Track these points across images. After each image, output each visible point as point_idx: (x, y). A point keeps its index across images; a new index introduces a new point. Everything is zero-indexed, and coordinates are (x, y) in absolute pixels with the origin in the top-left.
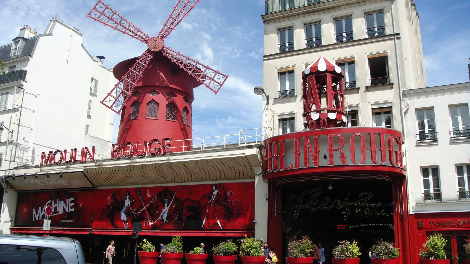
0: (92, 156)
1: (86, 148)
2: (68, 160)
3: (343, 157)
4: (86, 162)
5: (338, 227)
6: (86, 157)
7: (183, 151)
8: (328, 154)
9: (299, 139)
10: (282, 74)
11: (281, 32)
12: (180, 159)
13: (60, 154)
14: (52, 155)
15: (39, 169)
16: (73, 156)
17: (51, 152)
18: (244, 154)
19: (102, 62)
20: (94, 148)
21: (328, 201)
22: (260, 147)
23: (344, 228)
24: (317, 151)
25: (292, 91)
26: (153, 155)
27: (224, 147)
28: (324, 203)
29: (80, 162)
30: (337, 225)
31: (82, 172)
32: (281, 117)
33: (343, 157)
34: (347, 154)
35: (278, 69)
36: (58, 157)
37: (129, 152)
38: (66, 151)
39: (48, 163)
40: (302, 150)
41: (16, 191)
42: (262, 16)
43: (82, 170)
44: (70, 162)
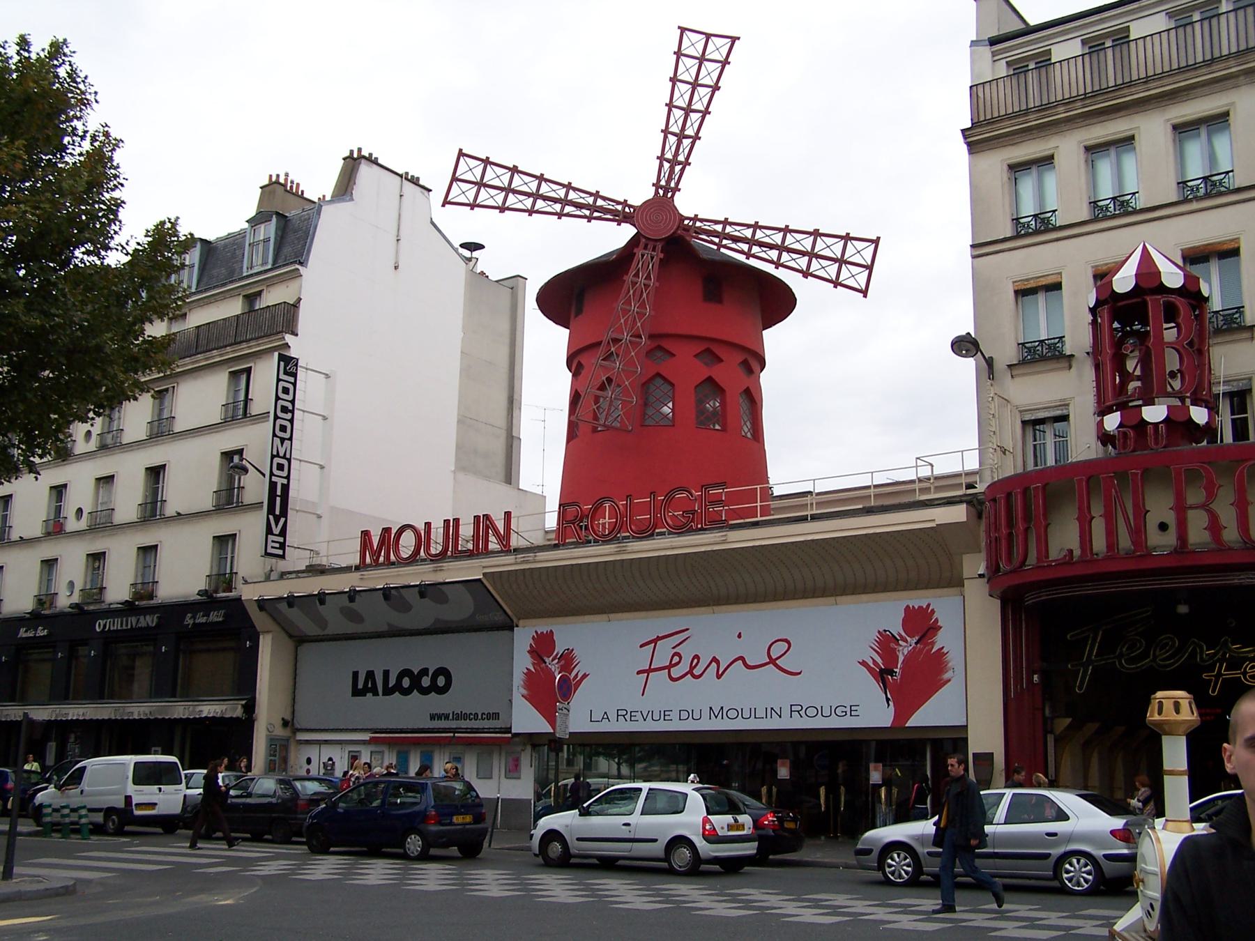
0: (504, 539)
1: (487, 517)
2: (436, 549)
3: (1215, 527)
4: (487, 553)
6: (487, 541)
7: (757, 517)
8: (1170, 518)
9: (1088, 482)
10: (1024, 293)
11: (1017, 173)
12: (754, 540)
13: (412, 533)
14: (389, 538)
15: (357, 575)
16: (451, 540)
17: (387, 531)
18: (934, 520)
19: (477, 259)
20: (508, 515)
21: (1170, 643)
22: (973, 502)
24: (1141, 513)
25: (1058, 342)
26: (681, 529)
27: (872, 504)
28: (1160, 651)
29: (470, 554)
31: (479, 580)
32: (1027, 418)
33: (1215, 527)
34: (1228, 516)
35: (1015, 282)
36: (407, 543)
37: (604, 524)
38: (428, 525)
39: (381, 559)
40: (1097, 509)
41: (291, 636)
42: (963, 131)
43: (481, 577)
44: (442, 556)
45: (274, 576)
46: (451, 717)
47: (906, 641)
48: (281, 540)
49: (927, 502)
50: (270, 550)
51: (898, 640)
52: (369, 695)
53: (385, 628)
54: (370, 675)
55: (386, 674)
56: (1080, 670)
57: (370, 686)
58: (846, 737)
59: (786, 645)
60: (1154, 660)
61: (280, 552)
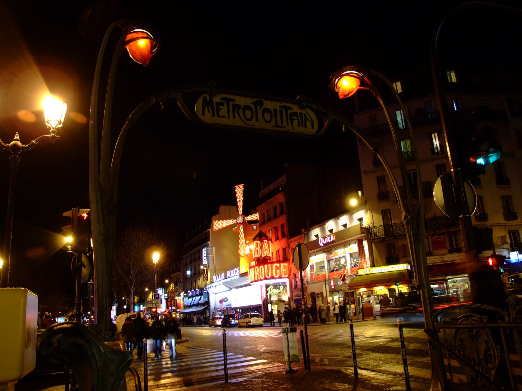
48: (207, 278)
50: (205, 280)
58: (255, 306)
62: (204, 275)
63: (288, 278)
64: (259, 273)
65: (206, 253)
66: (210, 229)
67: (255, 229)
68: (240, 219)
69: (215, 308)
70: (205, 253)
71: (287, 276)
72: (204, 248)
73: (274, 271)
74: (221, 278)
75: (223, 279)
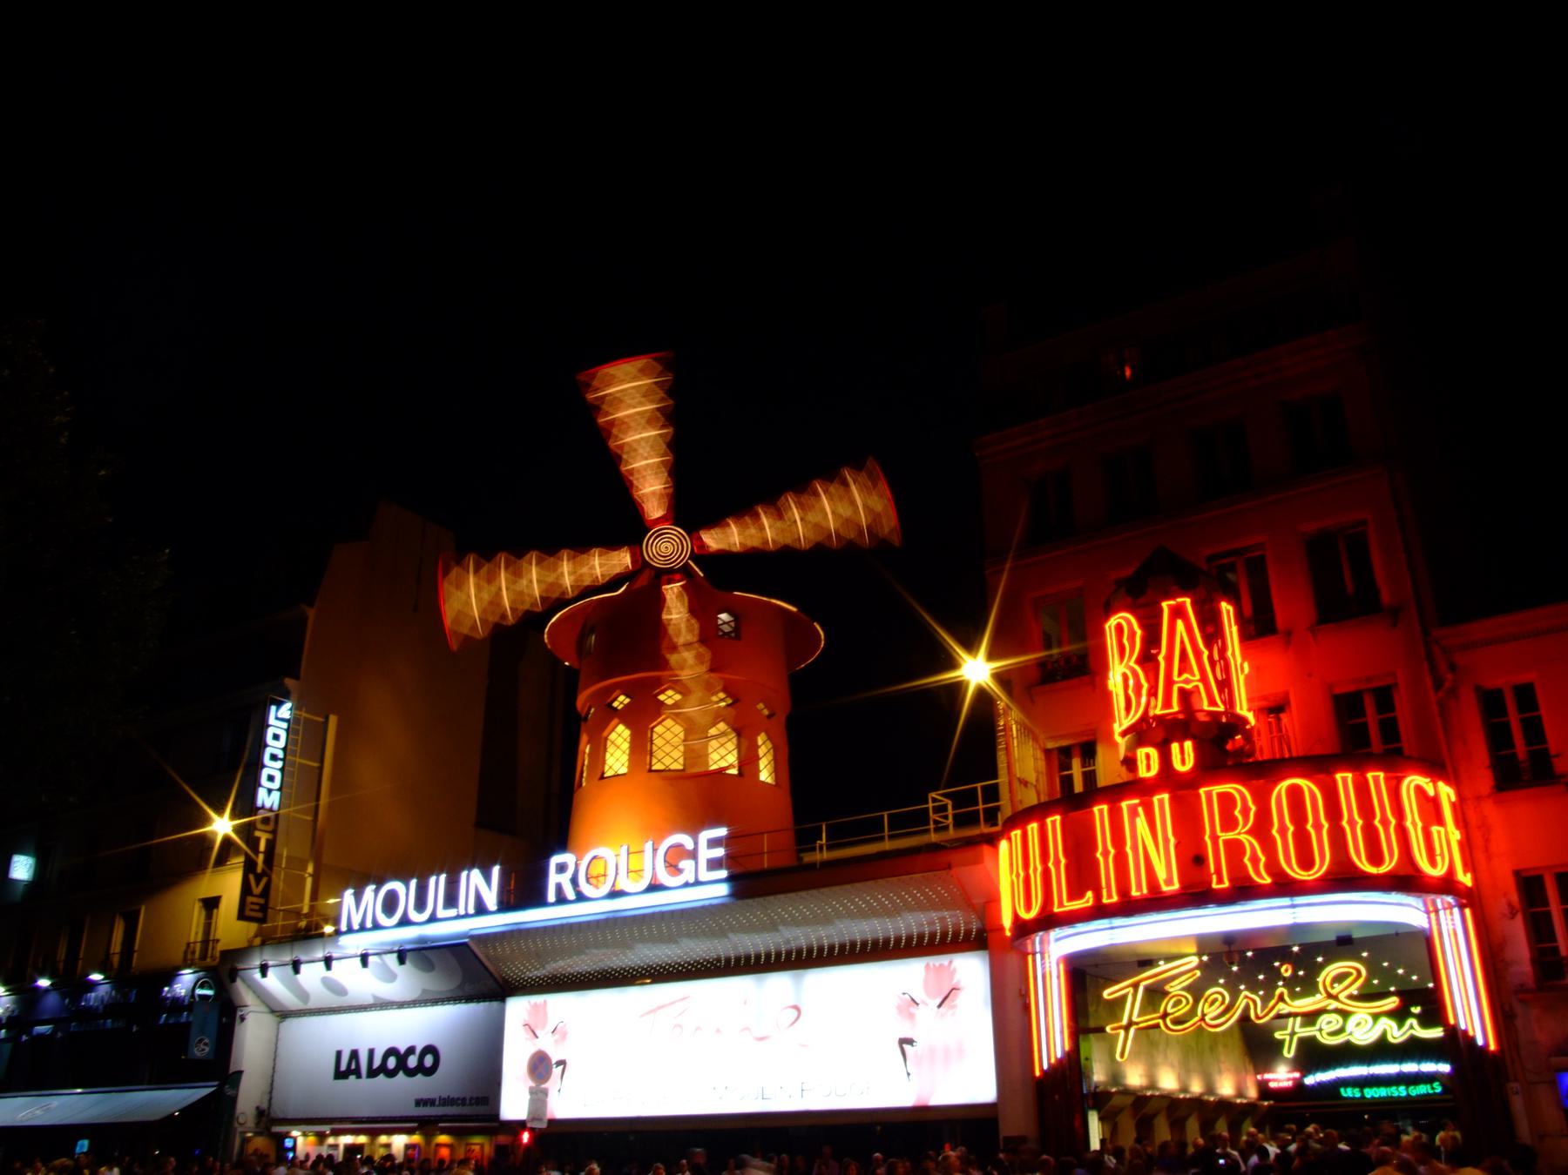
5: (1268, 1081)
23: (1290, 1083)
30: (1266, 1076)
41: (273, 1011)
45: (258, 941)
46: (437, 1103)
47: (927, 1005)
48: (262, 901)
49: (948, 845)
50: (248, 913)
51: (917, 1004)
52: (352, 1077)
53: (371, 1001)
54: (354, 1054)
55: (371, 1052)
56: (1118, 1035)
57: (353, 1067)
59: (795, 1013)
60: (1203, 1019)
61: (260, 915)
62: (251, 877)
63: (1467, 898)
64: (1261, 830)
65: (283, 735)
66: (311, 605)
67: (726, 629)
68: (667, 546)
69: (261, 1113)
70: (276, 737)
71: (1466, 879)
72: (279, 704)
73: (1414, 823)
74: (451, 900)
75: (467, 916)
